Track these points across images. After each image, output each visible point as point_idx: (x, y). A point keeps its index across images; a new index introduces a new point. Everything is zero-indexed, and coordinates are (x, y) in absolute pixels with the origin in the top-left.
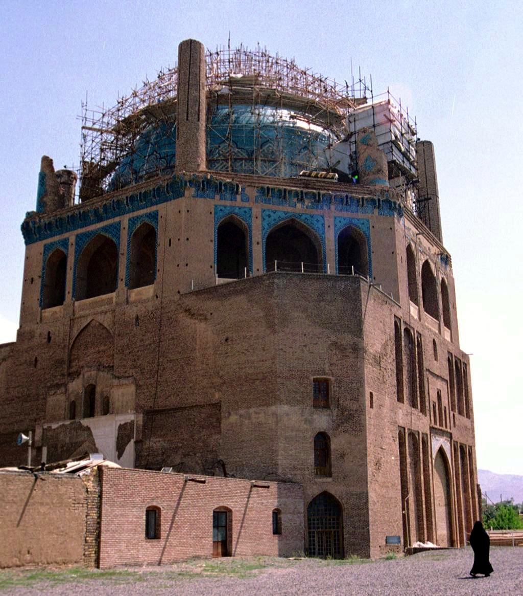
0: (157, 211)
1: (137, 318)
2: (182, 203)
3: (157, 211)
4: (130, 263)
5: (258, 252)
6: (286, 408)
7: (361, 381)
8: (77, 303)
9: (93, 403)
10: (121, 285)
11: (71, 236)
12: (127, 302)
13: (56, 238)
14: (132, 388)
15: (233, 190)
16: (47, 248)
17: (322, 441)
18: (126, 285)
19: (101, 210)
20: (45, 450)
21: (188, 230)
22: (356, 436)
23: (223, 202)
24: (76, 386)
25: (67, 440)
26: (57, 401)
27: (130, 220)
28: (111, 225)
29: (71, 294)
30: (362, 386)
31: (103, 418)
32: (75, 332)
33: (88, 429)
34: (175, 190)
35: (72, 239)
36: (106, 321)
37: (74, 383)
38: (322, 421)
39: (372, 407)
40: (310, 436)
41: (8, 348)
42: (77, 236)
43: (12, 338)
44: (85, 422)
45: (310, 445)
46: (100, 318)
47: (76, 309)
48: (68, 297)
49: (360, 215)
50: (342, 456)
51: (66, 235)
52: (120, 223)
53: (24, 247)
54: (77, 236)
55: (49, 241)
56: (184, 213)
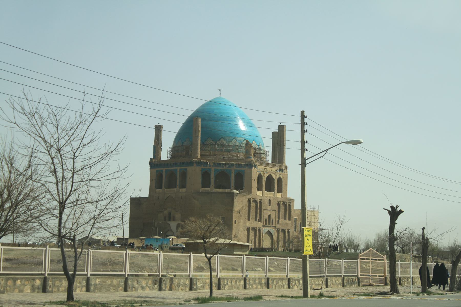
5: (212, 180)
7: (232, 218)
9: (170, 218)
10: (178, 187)
11: (164, 169)
14: (180, 215)
16: (157, 171)
20: (158, 228)
21: (194, 174)
24: (166, 212)
30: (232, 218)
33: (169, 224)
34: (191, 164)
35: (164, 170)
39: (235, 223)
42: (166, 170)
43: (148, 196)
44: (168, 222)
48: (163, 187)
49: (242, 169)
51: (162, 169)
55: (157, 169)
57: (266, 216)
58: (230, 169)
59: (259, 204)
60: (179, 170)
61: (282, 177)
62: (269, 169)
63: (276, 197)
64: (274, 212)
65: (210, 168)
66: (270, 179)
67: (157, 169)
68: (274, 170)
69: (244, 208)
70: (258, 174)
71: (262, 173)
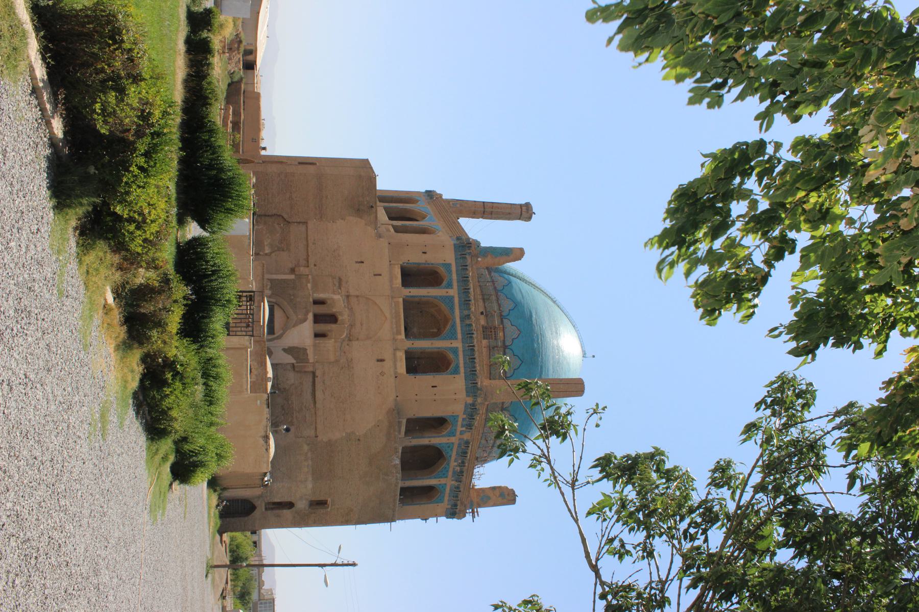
2: (462, 395)
6: (310, 486)
8: (401, 300)
10: (409, 344)
11: (454, 292)
12: (396, 350)
13: (454, 276)
15: (469, 426)
16: (448, 266)
17: (290, 505)
19: (468, 322)
20: (292, 277)
23: (460, 420)
25: (298, 300)
29: (408, 294)
31: (313, 336)
33: (305, 320)
38: (301, 505)
40: (292, 499)
42: (453, 297)
44: (310, 317)
47: (395, 300)
49: (446, 498)
51: (455, 284)
54: (453, 297)
55: (454, 268)
56: (454, 397)
58: (450, 473)
65: (458, 433)
67: (454, 268)
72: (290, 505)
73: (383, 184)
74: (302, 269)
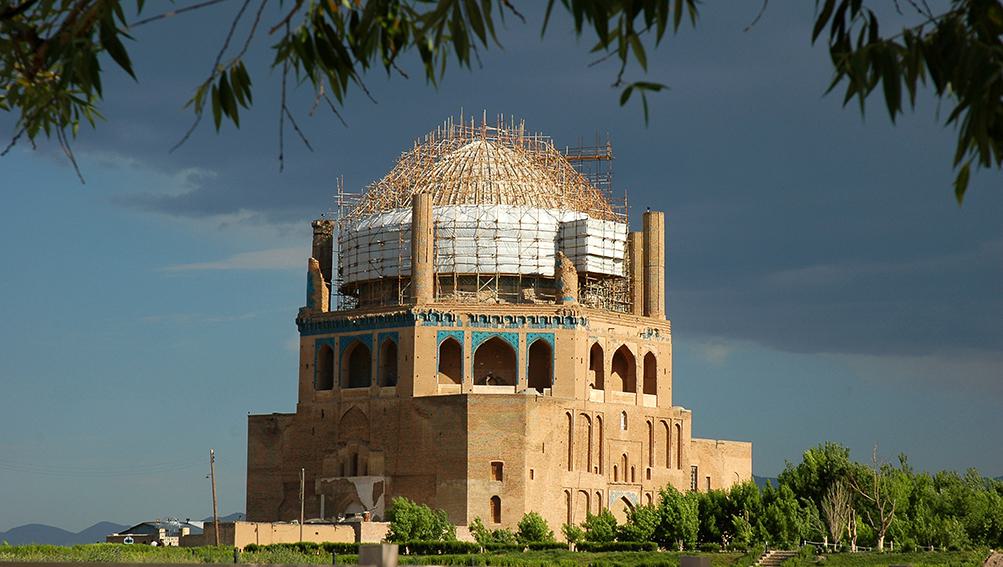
0: (397, 333)
1: (385, 410)
3: (397, 333)
4: (378, 367)
5: (468, 363)
8: (342, 391)
9: (357, 467)
10: (374, 383)
11: (337, 337)
12: (378, 395)
13: (325, 336)
14: (382, 459)
16: (317, 340)
17: (496, 500)
18: (378, 384)
22: (519, 498)
25: (339, 491)
26: (330, 461)
27: (379, 334)
28: (366, 335)
31: (364, 477)
32: (342, 414)
35: (337, 340)
36: (364, 408)
37: (343, 451)
38: (496, 488)
41: (291, 418)
45: (488, 502)
46: (359, 405)
48: (335, 385)
50: (508, 510)
51: (332, 335)
52: (371, 335)
53: (299, 338)
55: (319, 336)
57: (618, 461)
59: (597, 423)
60: (376, 336)
61: (655, 352)
62: (620, 330)
63: (642, 407)
64: (637, 446)
65: (461, 329)
66: (623, 360)
67: (319, 336)
68: (634, 332)
69: (555, 437)
70: (591, 344)
71: (602, 343)
72: (496, 500)
73: (284, 399)
74: (316, 488)
